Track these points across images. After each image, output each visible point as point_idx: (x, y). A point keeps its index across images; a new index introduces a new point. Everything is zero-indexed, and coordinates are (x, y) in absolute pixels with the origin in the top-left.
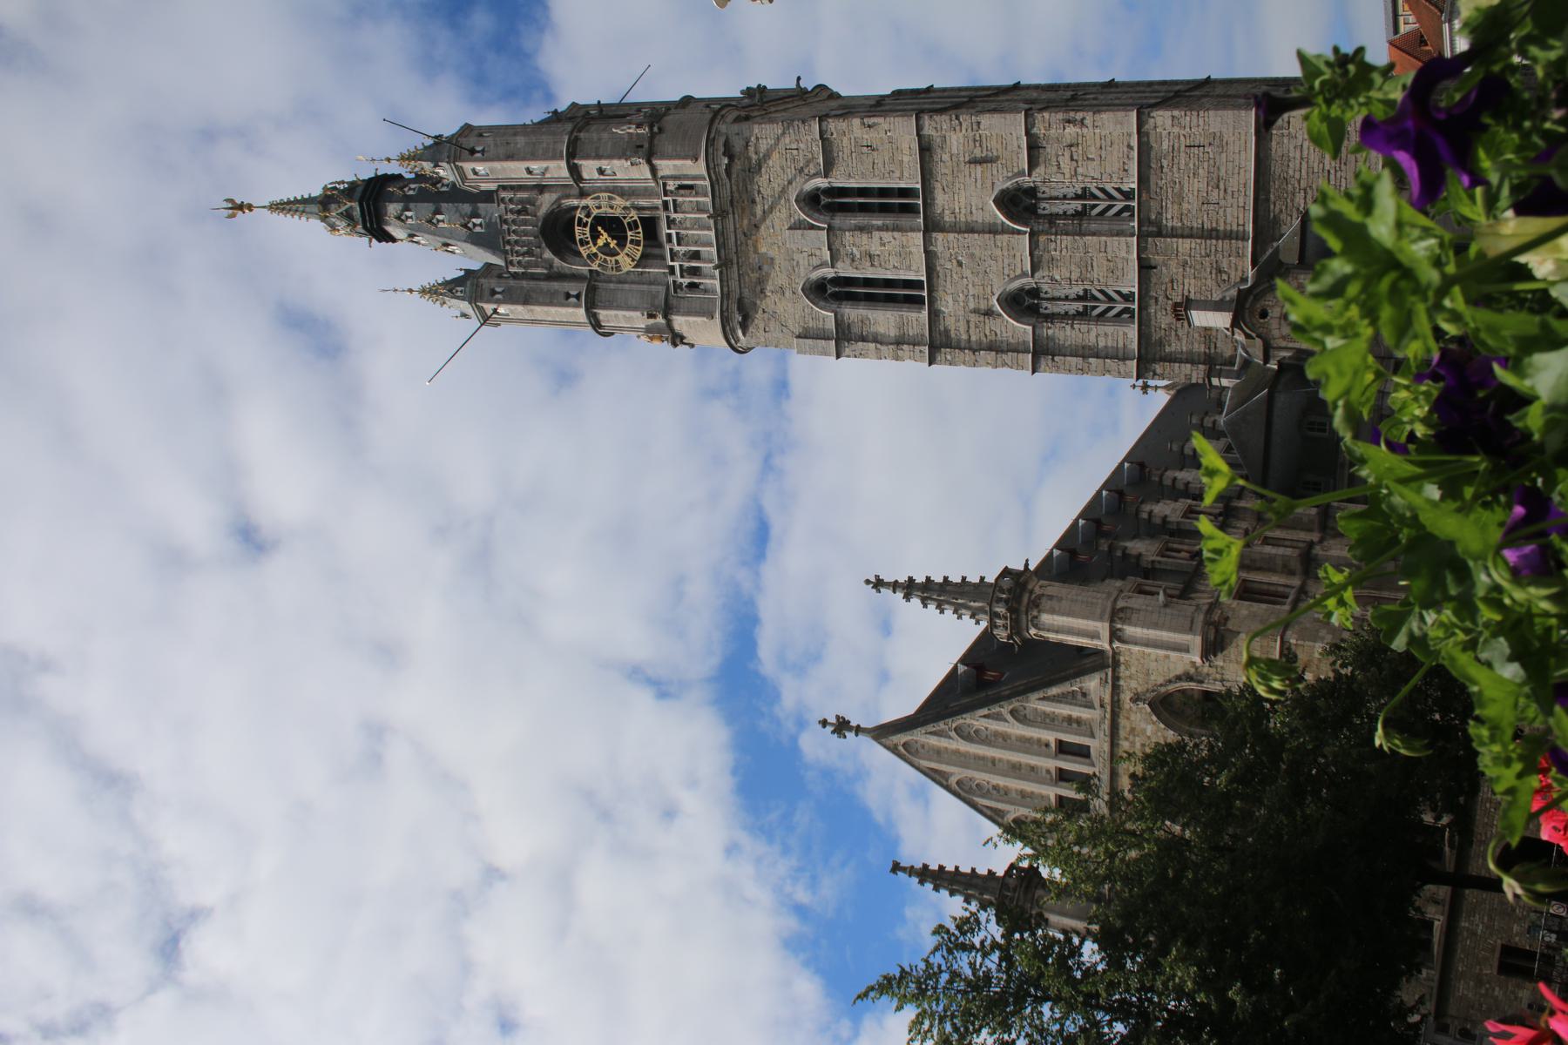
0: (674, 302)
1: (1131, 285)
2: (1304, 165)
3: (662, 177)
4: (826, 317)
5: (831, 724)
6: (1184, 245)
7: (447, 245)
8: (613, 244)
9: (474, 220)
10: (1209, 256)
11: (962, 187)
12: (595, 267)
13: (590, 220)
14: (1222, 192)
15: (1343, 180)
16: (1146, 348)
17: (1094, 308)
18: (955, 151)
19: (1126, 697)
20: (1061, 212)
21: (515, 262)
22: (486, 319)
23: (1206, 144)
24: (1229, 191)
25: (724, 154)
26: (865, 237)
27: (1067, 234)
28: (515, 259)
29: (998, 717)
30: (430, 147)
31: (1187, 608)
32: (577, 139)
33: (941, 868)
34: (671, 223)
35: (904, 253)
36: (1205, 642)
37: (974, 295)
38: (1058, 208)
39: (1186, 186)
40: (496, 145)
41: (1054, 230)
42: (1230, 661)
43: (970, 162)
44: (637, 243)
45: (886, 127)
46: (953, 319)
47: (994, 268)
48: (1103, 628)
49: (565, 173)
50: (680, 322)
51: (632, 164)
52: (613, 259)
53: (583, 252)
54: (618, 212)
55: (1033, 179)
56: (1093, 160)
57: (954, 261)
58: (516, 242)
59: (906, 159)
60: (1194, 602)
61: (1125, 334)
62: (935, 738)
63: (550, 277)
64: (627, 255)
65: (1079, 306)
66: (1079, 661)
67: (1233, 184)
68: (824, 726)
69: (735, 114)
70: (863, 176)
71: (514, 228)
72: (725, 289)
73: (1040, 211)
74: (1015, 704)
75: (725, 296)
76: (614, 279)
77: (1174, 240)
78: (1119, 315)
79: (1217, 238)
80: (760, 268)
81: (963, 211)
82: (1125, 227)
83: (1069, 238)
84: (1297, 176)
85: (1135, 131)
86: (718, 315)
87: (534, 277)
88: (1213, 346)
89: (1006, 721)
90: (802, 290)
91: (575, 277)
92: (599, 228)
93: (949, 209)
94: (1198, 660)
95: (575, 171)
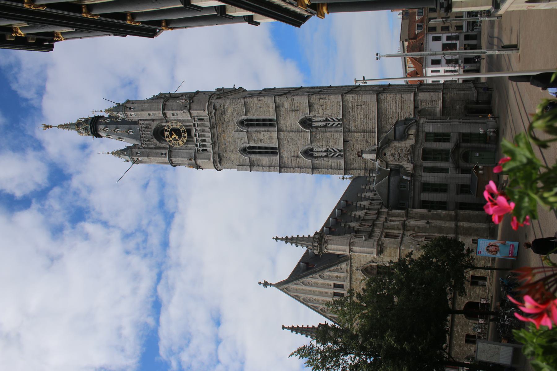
0: (197, 155)
1: (341, 147)
2: (391, 111)
3: (193, 116)
4: (246, 159)
5: (262, 283)
6: (357, 135)
7: (120, 138)
8: (177, 137)
9: (130, 130)
10: (364, 138)
12: (171, 144)
13: (169, 130)
14: (367, 119)
16: (346, 166)
17: (330, 154)
18: (286, 107)
19: (354, 269)
20: (319, 125)
21: (144, 144)
22: (134, 162)
23: (362, 104)
25: (214, 109)
26: (259, 134)
27: (321, 132)
28: (144, 142)
29: (315, 278)
30: (116, 107)
31: (371, 242)
32: (165, 104)
33: (298, 326)
34: (196, 130)
35: (271, 139)
36: (377, 250)
38: (318, 124)
39: (357, 117)
40: (138, 106)
41: (317, 131)
42: (385, 256)
43: (291, 111)
44: (185, 137)
45: (265, 100)
46: (287, 159)
47: (299, 143)
48: (347, 248)
49: (161, 115)
50: (199, 162)
51: (184, 112)
52: (177, 142)
53: (167, 140)
54: (178, 127)
55: (310, 115)
56: (328, 110)
57: (287, 141)
58: (145, 137)
59: (271, 110)
60: (373, 239)
61: (340, 162)
62: (296, 285)
63: (155, 148)
64: (182, 141)
65: (326, 154)
66: (337, 259)
67: (371, 116)
68: (260, 284)
69: (216, 97)
70: (258, 115)
71: (144, 132)
72: (214, 151)
73: (313, 125)
74: (321, 273)
75: (214, 153)
76: (177, 148)
77: (354, 133)
78: (338, 156)
79: (367, 132)
80: (225, 144)
81: (289, 125)
82: (339, 130)
83: (322, 133)
84: (389, 113)
86: (212, 159)
87: (150, 148)
88: (366, 164)
89: (318, 278)
90: (239, 151)
91: (164, 148)
92: (173, 132)
93: (285, 125)
94: (375, 256)
95: (164, 114)
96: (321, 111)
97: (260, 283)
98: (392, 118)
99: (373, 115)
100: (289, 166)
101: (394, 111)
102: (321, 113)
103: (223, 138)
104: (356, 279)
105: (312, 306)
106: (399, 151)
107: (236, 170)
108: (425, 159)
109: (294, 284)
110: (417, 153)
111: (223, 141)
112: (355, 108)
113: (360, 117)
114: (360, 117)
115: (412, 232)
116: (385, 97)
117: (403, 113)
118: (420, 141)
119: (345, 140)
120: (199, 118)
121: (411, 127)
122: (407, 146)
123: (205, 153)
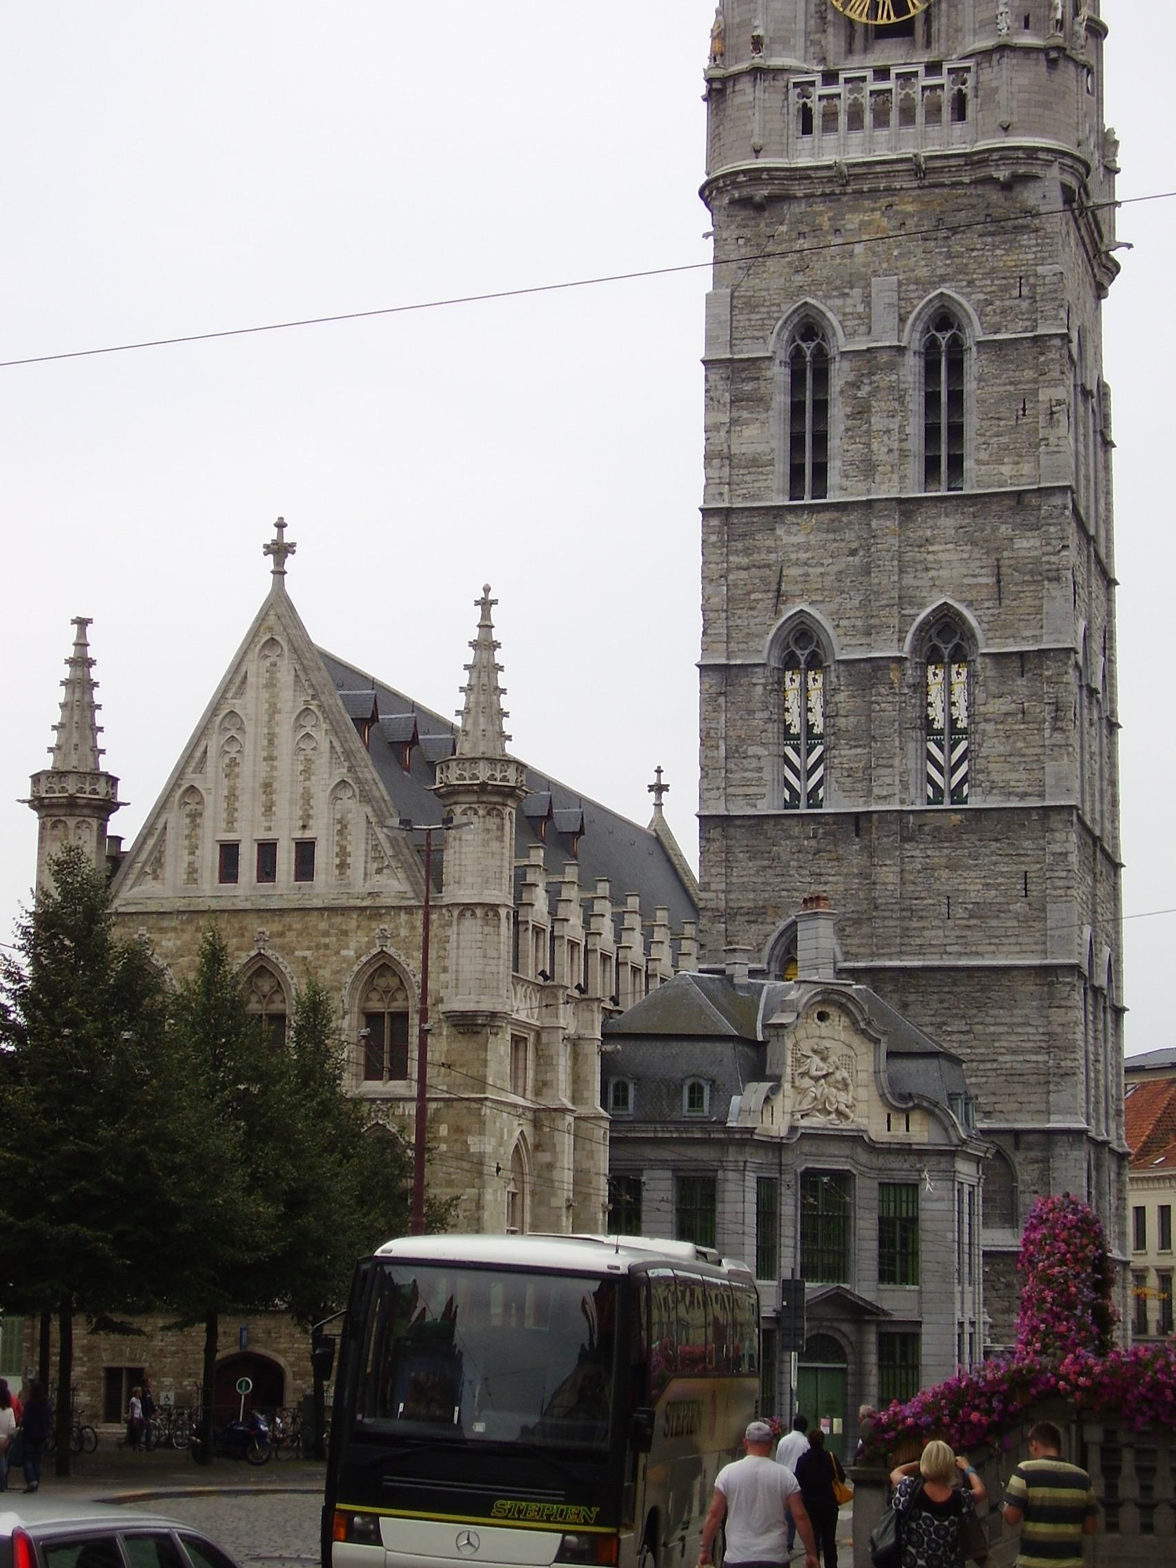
1: (836, 803)
5: (281, 534)
11: (965, 556)
15: (985, 1079)
16: (740, 827)
17: (797, 750)
18: (1019, 543)
20: (930, 699)
24: (969, 933)
35: (868, 468)
37: (807, 575)
38: (936, 695)
39: (973, 874)
55: (979, 660)
57: (854, 545)
59: (1006, 470)
69: (1074, 184)
78: (788, 784)
81: (930, 557)
82: (912, 790)
84: (989, 1020)
85: (1046, 804)
86: (761, 163)
90: (806, 303)
96: (998, 707)
97: (281, 525)
98: (968, 1032)
99: (980, 949)
100: (736, 552)
101: (1005, 1044)
102: (989, 708)
103: (870, 223)
104: (345, 933)
105: (205, 752)
106: (838, 1076)
107: (710, 288)
108: (809, 1179)
109: (297, 676)
110: (832, 1149)
111: (853, 220)
112: (1015, 868)
113: (973, 888)
114: (972, 887)
115: (530, 1140)
116: (1063, 1003)
117: (991, 1080)
118: (880, 1161)
119: (863, 823)
120: (970, 97)
121: (940, 1121)
122: (861, 1107)
123: (795, 125)
